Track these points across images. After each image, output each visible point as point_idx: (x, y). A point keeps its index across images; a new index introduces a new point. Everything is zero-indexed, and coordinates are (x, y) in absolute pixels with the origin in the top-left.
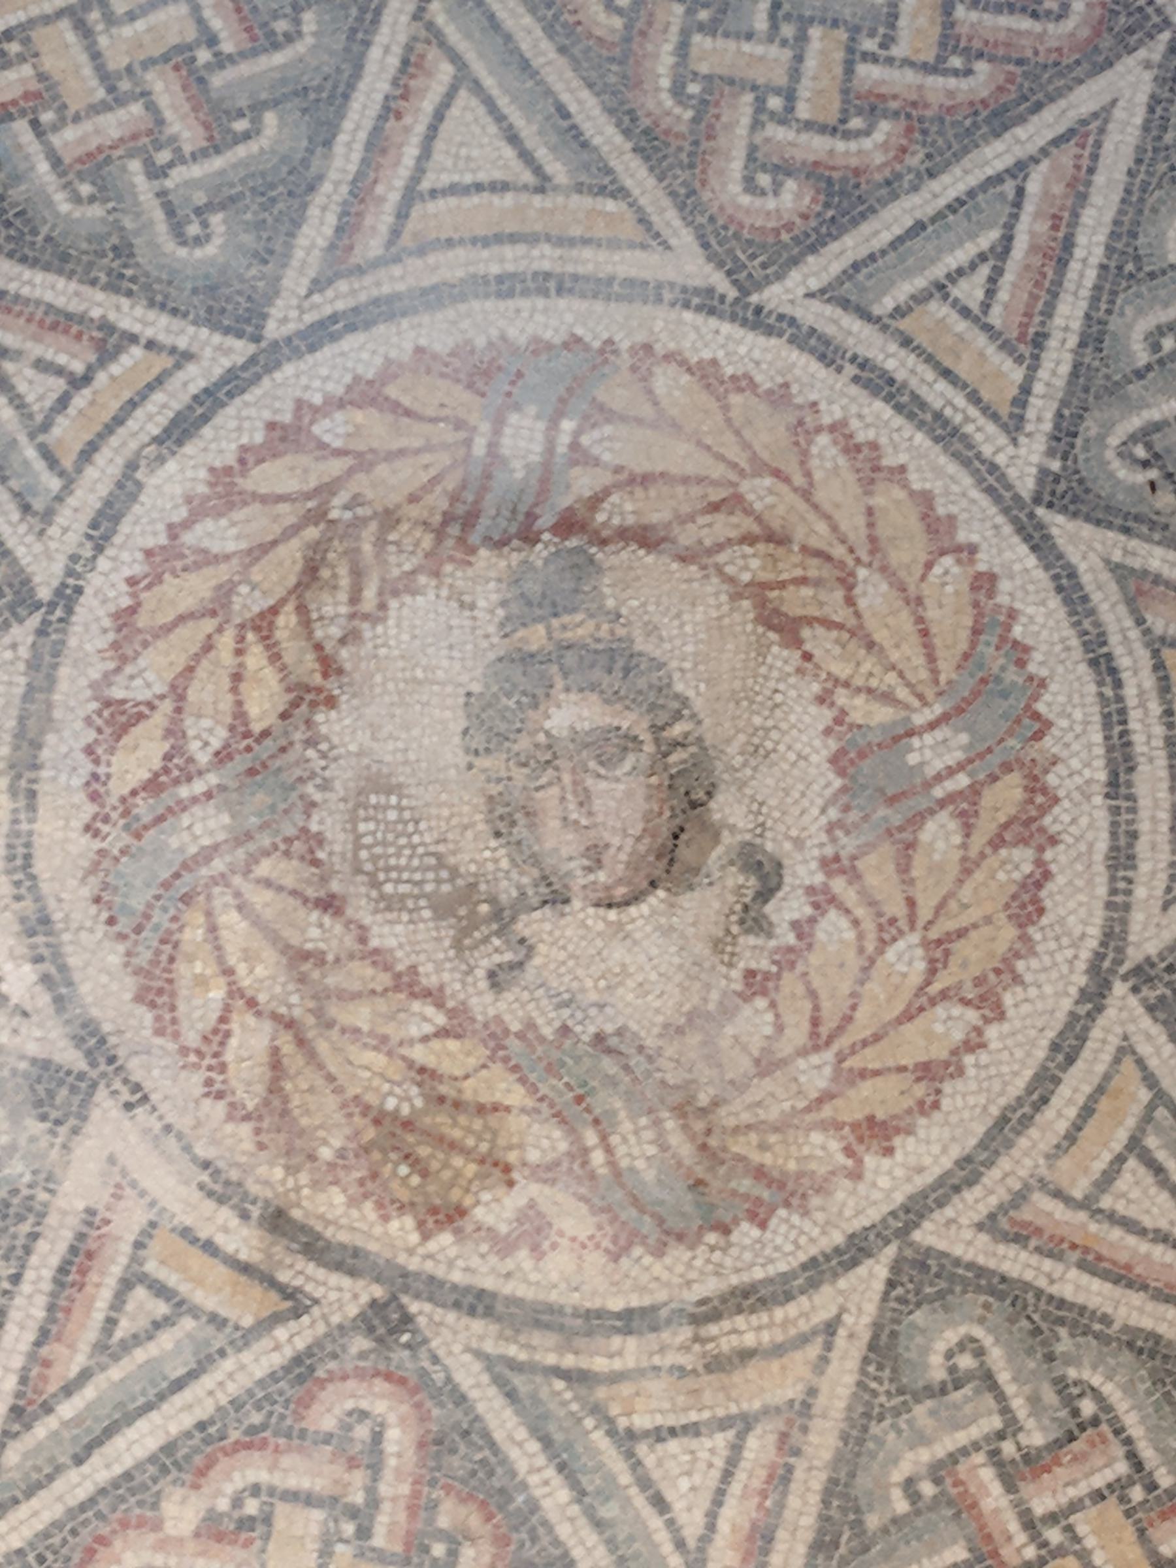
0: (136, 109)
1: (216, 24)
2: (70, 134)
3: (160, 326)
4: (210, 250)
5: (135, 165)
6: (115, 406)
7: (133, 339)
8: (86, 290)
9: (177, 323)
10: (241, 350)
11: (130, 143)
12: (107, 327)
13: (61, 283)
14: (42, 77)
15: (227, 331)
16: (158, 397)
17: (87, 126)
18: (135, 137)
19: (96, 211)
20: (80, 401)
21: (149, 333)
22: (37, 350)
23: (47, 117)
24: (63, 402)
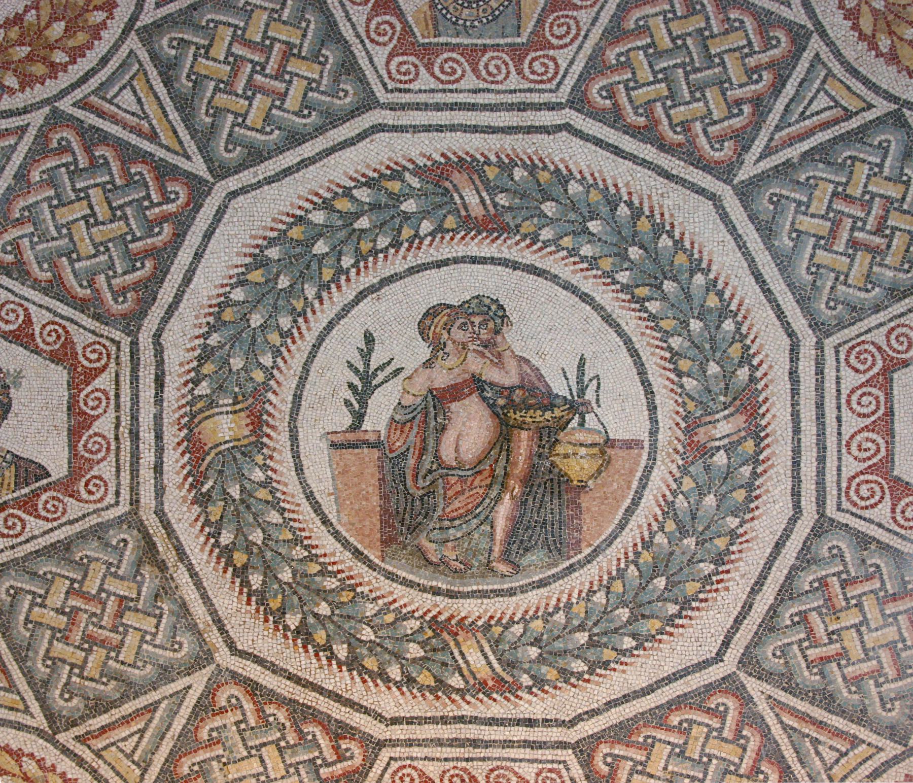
0: (874, 662)
1: (906, 635)
2: (850, 669)
3: (873, 738)
4: (894, 713)
5: (871, 682)
6: (854, 764)
7: (864, 742)
8: (850, 724)
9: (879, 738)
10: (900, 749)
11: (872, 674)
12: (855, 737)
13: (841, 720)
14: (843, 648)
15: (896, 742)
16: (870, 762)
17: (857, 667)
18: (873, 672)
19: (856, 697)
20: (843, 761)
21: (869, 740)
22: (831, 743)
23: (843, 662)
24: (837, 761)
